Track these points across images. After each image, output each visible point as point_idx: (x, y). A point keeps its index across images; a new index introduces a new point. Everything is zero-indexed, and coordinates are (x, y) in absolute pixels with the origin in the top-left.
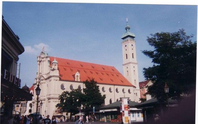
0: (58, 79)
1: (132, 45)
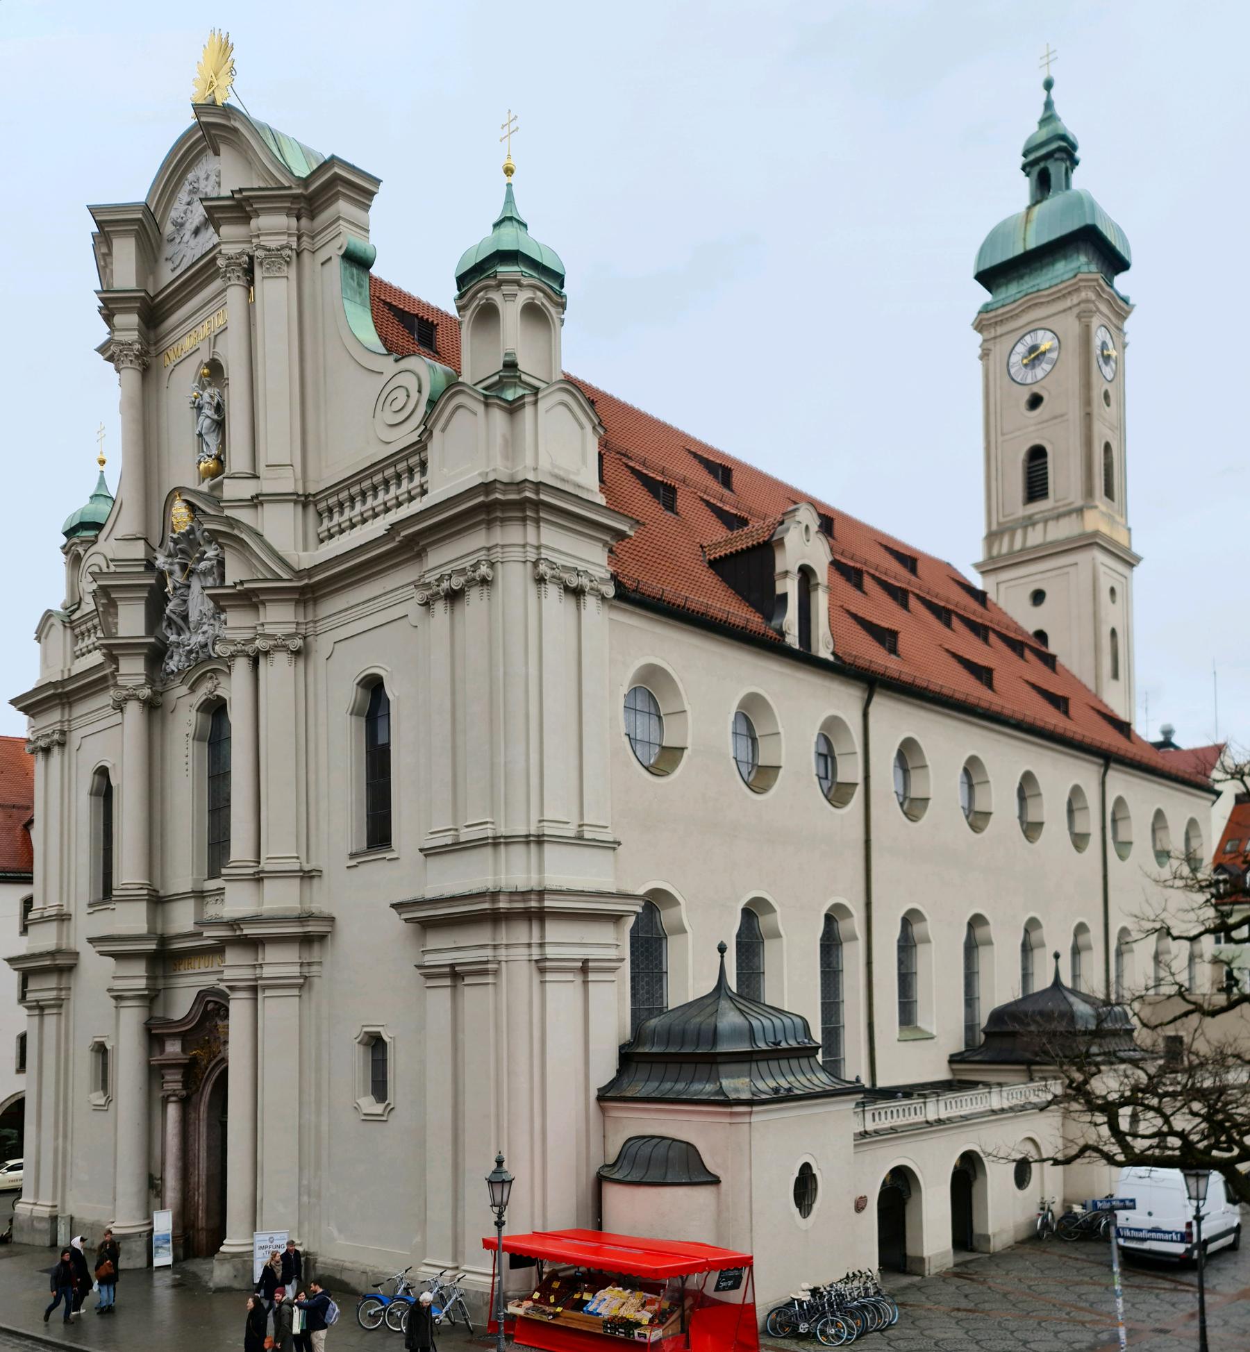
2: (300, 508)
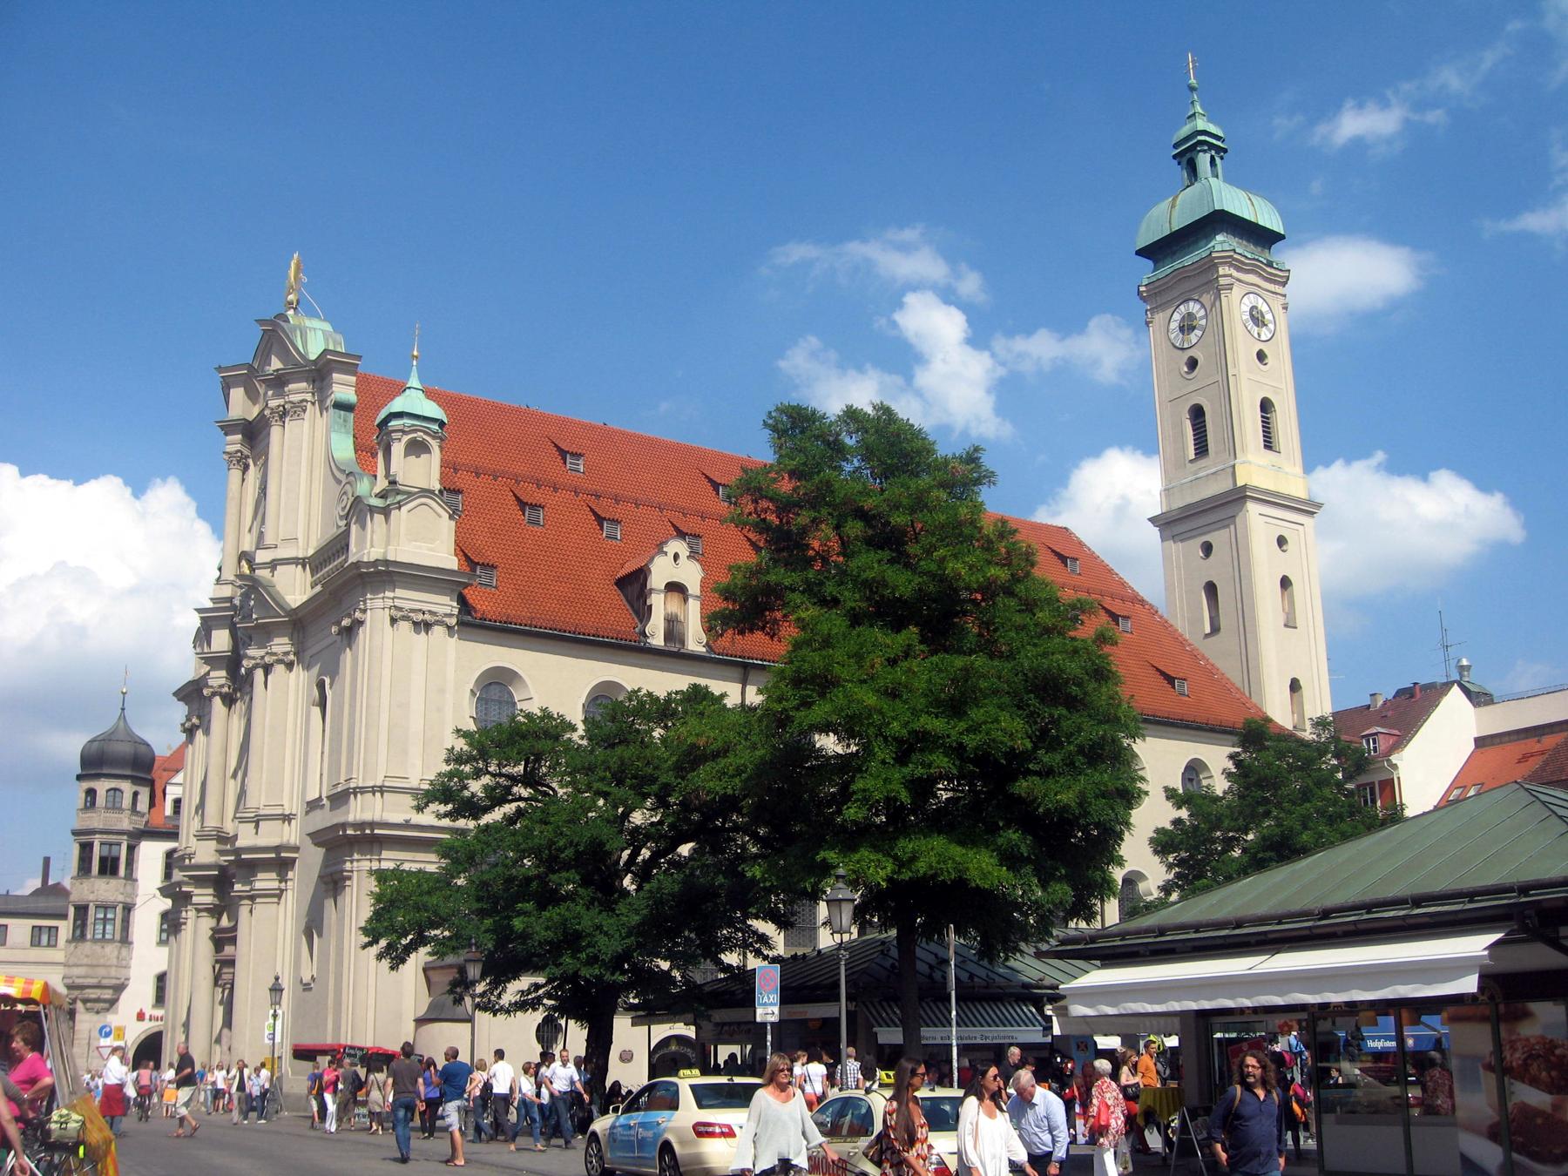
0: (445, 605)
1: (1257, 319)
2: (300, 566)
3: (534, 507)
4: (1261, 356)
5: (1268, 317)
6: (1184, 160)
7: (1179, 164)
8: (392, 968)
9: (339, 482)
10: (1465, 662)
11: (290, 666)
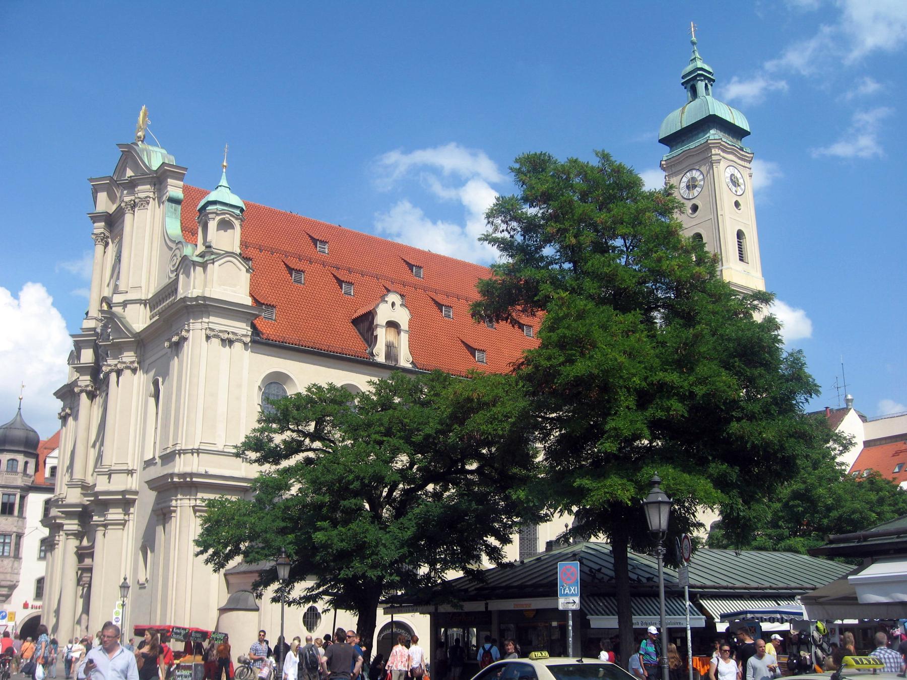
0: (242, 329)
1: (734, 182)
2: (142, 305)
3: (299, 271)
4: (737, 204)
5: (741, 181)
6: (689, 86)
7: (685, 88)
8: (215, 571)
9: (170, 249)
10: (849, 397)
11: (134, 371)
